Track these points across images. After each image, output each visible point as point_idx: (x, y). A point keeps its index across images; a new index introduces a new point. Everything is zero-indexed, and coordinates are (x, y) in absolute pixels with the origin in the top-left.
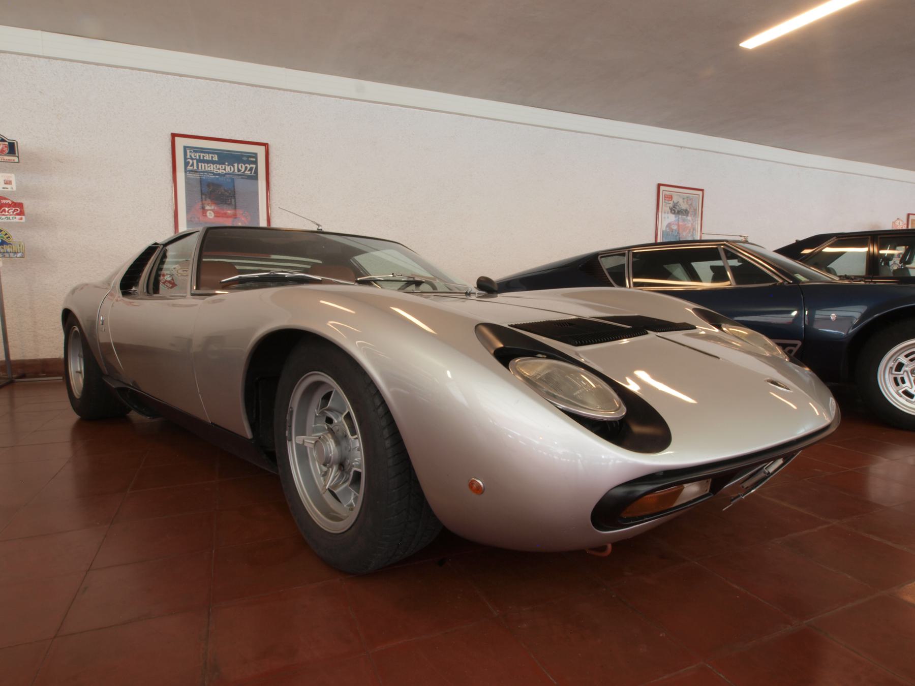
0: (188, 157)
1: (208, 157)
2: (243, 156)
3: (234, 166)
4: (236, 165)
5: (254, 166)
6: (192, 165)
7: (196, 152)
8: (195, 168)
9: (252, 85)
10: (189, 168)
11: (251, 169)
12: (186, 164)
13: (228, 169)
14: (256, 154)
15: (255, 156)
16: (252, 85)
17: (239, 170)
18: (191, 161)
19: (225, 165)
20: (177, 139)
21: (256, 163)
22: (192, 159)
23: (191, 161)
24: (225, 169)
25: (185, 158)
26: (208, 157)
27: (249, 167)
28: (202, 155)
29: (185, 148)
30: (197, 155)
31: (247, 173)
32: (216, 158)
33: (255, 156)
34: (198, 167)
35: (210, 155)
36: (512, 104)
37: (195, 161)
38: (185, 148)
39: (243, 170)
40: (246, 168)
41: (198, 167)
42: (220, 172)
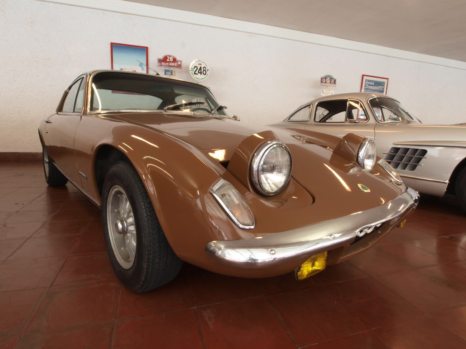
0: (366, 83)
1: (371, 84)
2: (381, 83)
3: (378, 87)
4: (378, 86)
5: (383, 87)
6: (367, 87)
7: (368, 81)
8: (367, 87)
9: (377, 54)
10: (366, 87)
11: (383, 88)
12: (365, 86)
13: (376, 88)
14: (384, 82)
15: (384, 83)
16: (377, 54)
17: (379, 89)
18: (366, 85)
19: (375, 86)
20: (364, 77)
21: (384, 86)
22: (367, 84)
23: (366, 85)
24: (375, 88)
25: (365, 84)
26: (371, 84)
27: (382, 87)
28: (370, 83)
29: (366, 80)
30: (369, 82)
31: (381, 89)
32: (373, 84)
33: (384, 83)
34: (368, 87)
35: (372, 83)
36: (317, 34)
37: (368, 85)
38: (366, 80)
39: (380, 88)
40: (381, 87)
41: (368, 87)
42: (374, 89)
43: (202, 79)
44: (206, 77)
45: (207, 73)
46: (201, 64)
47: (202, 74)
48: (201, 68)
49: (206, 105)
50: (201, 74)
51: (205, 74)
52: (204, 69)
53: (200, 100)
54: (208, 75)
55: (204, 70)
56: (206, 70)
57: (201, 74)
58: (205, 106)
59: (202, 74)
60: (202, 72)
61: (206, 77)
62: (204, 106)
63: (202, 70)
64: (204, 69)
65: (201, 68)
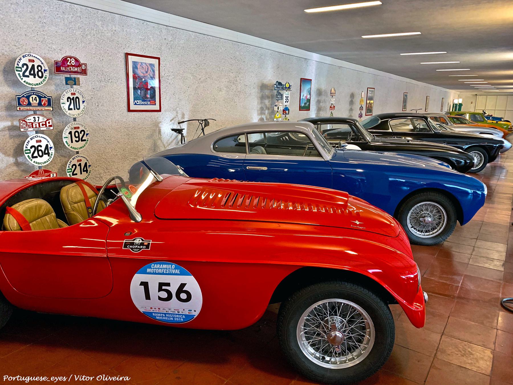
43: (37, 84)
44: (44, 80)
45: (44, 75)
46: (33, 61)
47: (37, 76)
48: (33, 66)
49: (49, 124)
50: (35, 77)
51: (41, 77)
52: (40, 68)
53: (39, 117)
54: (46, 78)
55: (39, 71)
56: (43, 71)
57: (35, 77)
58: (48, 126)
59: (37, 76)
60: (36, 73)
61: (44, 80)
62: (46, 126)
63: (36, 70)
64: (40, 68)
65: (33, 66)
